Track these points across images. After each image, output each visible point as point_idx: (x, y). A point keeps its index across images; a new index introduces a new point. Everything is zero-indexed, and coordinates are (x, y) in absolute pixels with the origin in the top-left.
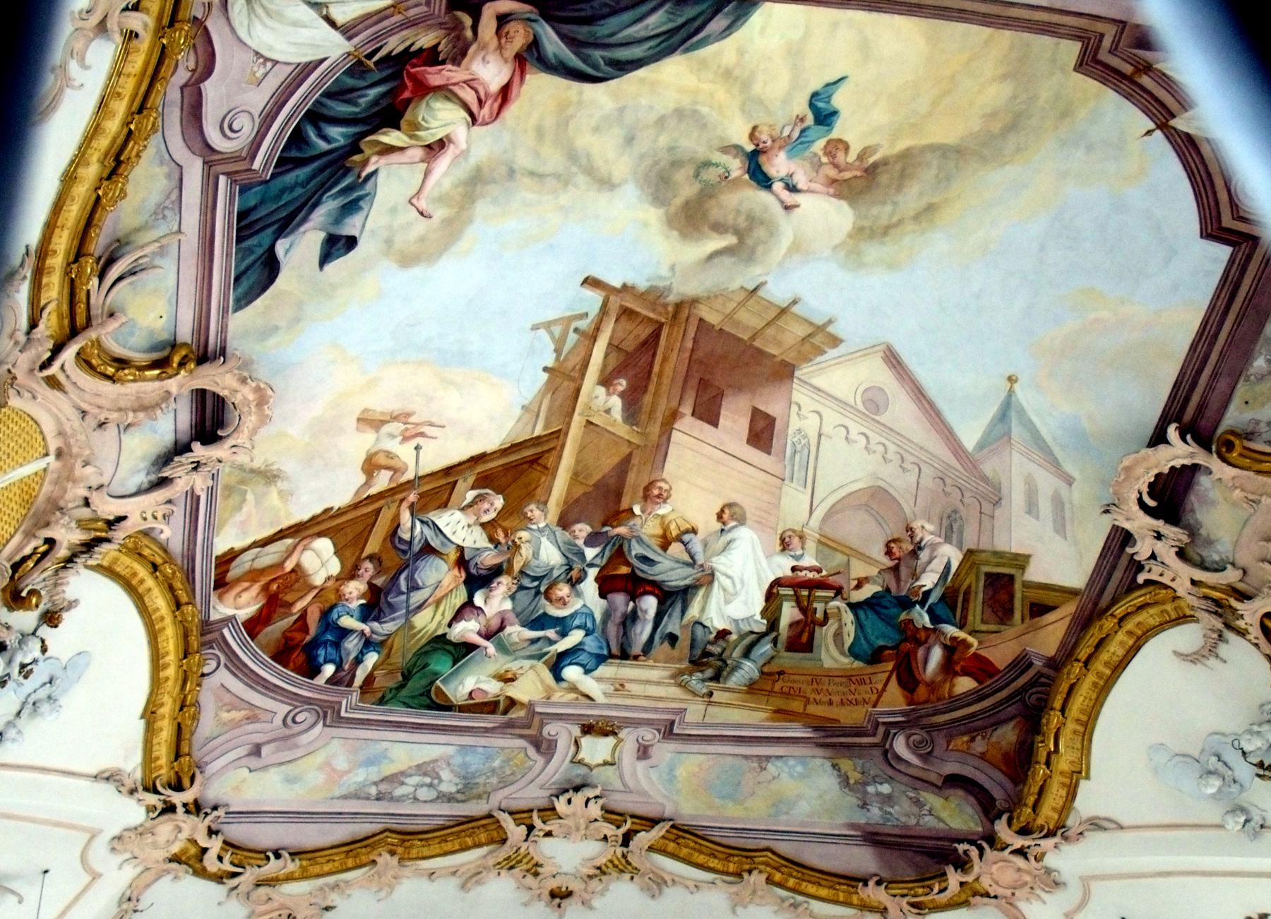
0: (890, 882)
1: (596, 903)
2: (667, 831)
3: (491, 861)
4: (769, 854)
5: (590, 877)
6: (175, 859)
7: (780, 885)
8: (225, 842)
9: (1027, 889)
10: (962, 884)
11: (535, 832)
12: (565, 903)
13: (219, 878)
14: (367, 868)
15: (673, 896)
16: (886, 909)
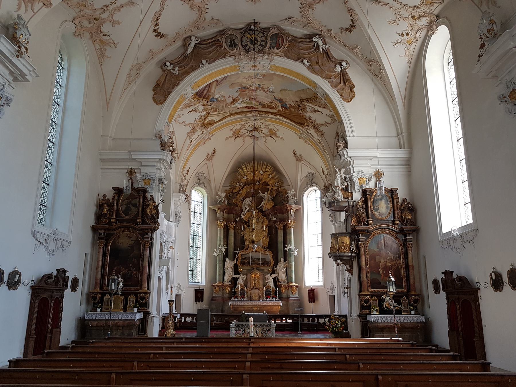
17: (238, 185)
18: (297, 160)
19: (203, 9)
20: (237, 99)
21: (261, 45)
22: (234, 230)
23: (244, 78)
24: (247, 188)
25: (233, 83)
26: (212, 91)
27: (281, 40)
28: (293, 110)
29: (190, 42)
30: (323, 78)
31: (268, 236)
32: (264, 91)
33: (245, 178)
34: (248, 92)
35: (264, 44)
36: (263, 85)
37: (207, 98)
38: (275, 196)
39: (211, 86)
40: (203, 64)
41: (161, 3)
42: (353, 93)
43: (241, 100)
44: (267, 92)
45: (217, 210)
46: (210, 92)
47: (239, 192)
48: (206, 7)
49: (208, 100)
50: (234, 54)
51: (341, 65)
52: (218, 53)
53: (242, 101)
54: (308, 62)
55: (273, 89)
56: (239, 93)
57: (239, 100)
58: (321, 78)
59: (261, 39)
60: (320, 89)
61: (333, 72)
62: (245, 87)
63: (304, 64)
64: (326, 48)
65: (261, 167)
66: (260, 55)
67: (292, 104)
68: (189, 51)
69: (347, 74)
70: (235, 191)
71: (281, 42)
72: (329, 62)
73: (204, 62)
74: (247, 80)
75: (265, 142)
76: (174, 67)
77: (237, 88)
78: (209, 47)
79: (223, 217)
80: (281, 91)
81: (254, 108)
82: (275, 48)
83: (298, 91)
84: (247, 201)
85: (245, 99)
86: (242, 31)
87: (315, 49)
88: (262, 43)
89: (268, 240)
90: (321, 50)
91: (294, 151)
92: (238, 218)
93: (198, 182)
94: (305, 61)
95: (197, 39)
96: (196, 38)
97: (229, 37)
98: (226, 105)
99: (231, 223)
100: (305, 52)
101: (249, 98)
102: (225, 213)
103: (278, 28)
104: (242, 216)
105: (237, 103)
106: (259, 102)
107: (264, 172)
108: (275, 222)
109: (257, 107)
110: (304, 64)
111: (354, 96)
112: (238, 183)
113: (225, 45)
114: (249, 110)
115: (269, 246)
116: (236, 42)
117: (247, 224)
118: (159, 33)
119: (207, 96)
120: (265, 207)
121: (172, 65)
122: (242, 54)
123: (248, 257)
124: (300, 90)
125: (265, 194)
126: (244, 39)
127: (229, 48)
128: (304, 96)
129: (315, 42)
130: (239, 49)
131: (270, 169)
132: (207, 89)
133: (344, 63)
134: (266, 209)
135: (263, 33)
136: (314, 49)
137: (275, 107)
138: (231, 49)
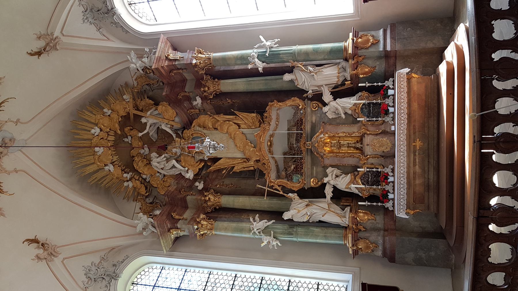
17: (131, 184)
18: (55, 48)
22: (223, 193)
24: (140, 164)
31: (233, 114)
33: (111, 168)
38: (151, 102)
45: (173, 237)
47: (147, 181)
65: (83, 132)
70: (143, 191)
75: (17, 122)
79: (189, 223)
84: (157, 165)
89: (245, 114)
91: (31, 54)
92: (197, 184)
93: (107, 279)
99: (206, 201)
102: (180, 216)
104: (190, 175)
107: (96, 125)
108: (204, 99)
112: (126, 184)
115: (257, 113)
117: (209, 164)
120: (172, 123)
123: (284, 162)
125: (146, 124)
131: (92, 112)
134: (177, 119)
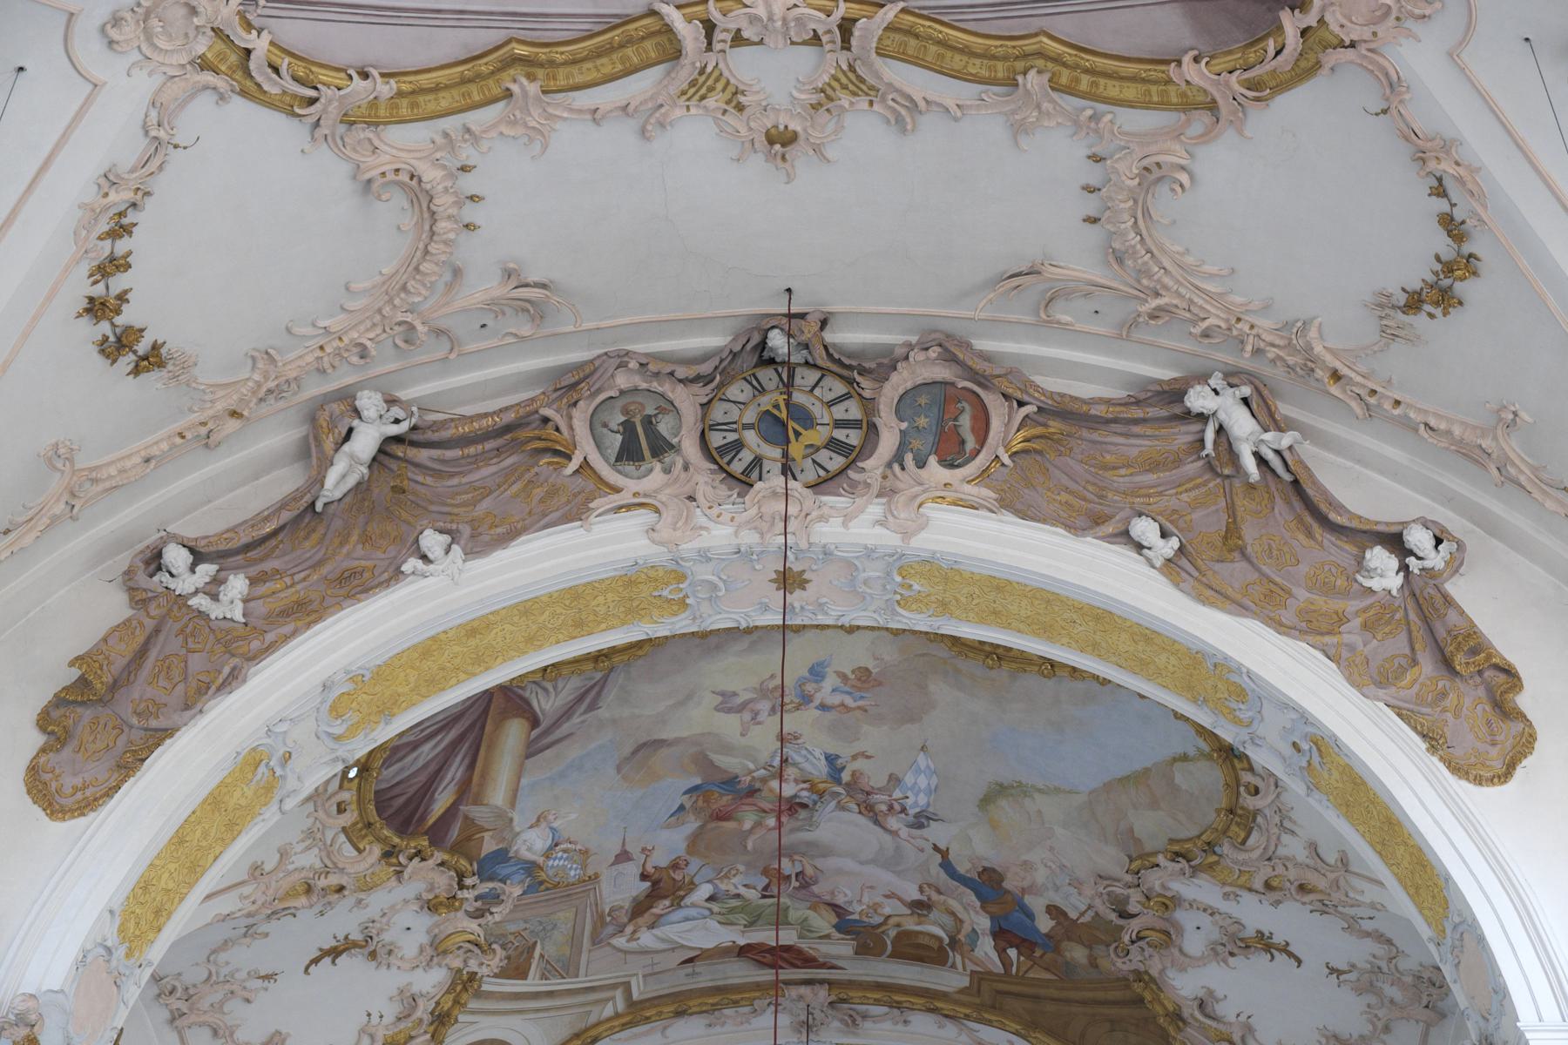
0: (1212, 57)
1: (831, 153)
2: (895, 16)
3: (674, 90)
4: (1045, 40)
5: (816, 107)
6: (204, 65)
7: (1070, 91)
8: (272, 43)
9: (1391, 21)
10: (1304, 32)
11: (718, 35)
12: (791, 151)
13: (288, 106)
14: (501, 104)
15: (931, 126)
16: (1214, 101)
19: (443, 202)
20: (678, 876)
21: (834, 445)
23: (727, 703)
25: (644, 745)
26: (498, 795)
27: (974, 418)
28: (1077, 953)
29: (351, 430)
30: (1280, 627)
32: (868, 809)
34: (758, 824)
35: (853, 437)
36: (859, 764)
37: (455, 849)
39: (490, 747)
40: (424, 558)
41: (154, 114)
42: (1518, 727)
43: (705, 890)
44: (893, 823)
46: (477, 801)
48: (469, 184)
49: (463, 863)
50: (646, 495)
51: (1395, 542)
52: (538, 492)
53: (711, 899)
54: (1164, 535)
55: (929, 792)
56: (692, 825)
57: (692, 886)
58: (1269, 633)
59: (839, 412)
60: (1268, 710)
61: (1346, 594)
62: (730, 782)
63: (1139, 547)
64: (1278, 452)
66: (825, 498)
67: (1075, 905)
68: (340, 476)
69: (1448, 601)
71: (973, 430)
72: (1310, 534)
73: (432, 541)
74: (747, 716)
76: (217, 581)
77: (674, 786)
78: (477, 461)
80: (986, 801)
81: (809, 961)
82: (933, 460)
83: (1108, 787)
85: (734, 884)
86: (705, 368)
87: (1210, 467)
88: (840, 434)
90: (1250, 464)
94: (1145, 529)
95: (401, 414)
96: (391, 401)
97: (620, 403)
98: (600, 921)
100: (1138, 479)
101: (765, 872)
103: (950, 348)
105: (679, 914)
106: (834, 907)
109: (825, 950)
110: (1139, 547)
111: (1526, 743)
113: (586, 448)
114: (767, 975)
116: (664, 427)
118: (128, 329)
119: (454, 833)
121: (206, 570)
122: (700, 497)
124: (1124, 781)
126: (718, 413)
127: (613, 466)
128: (1152, 826)
129: (1203, 418)
130: (686, 468)
132: (456, 771)
133: (1419, 538)
135: (850, 382)
136: (1200, 463)
137: (954, 942)
138: (630, 468)
